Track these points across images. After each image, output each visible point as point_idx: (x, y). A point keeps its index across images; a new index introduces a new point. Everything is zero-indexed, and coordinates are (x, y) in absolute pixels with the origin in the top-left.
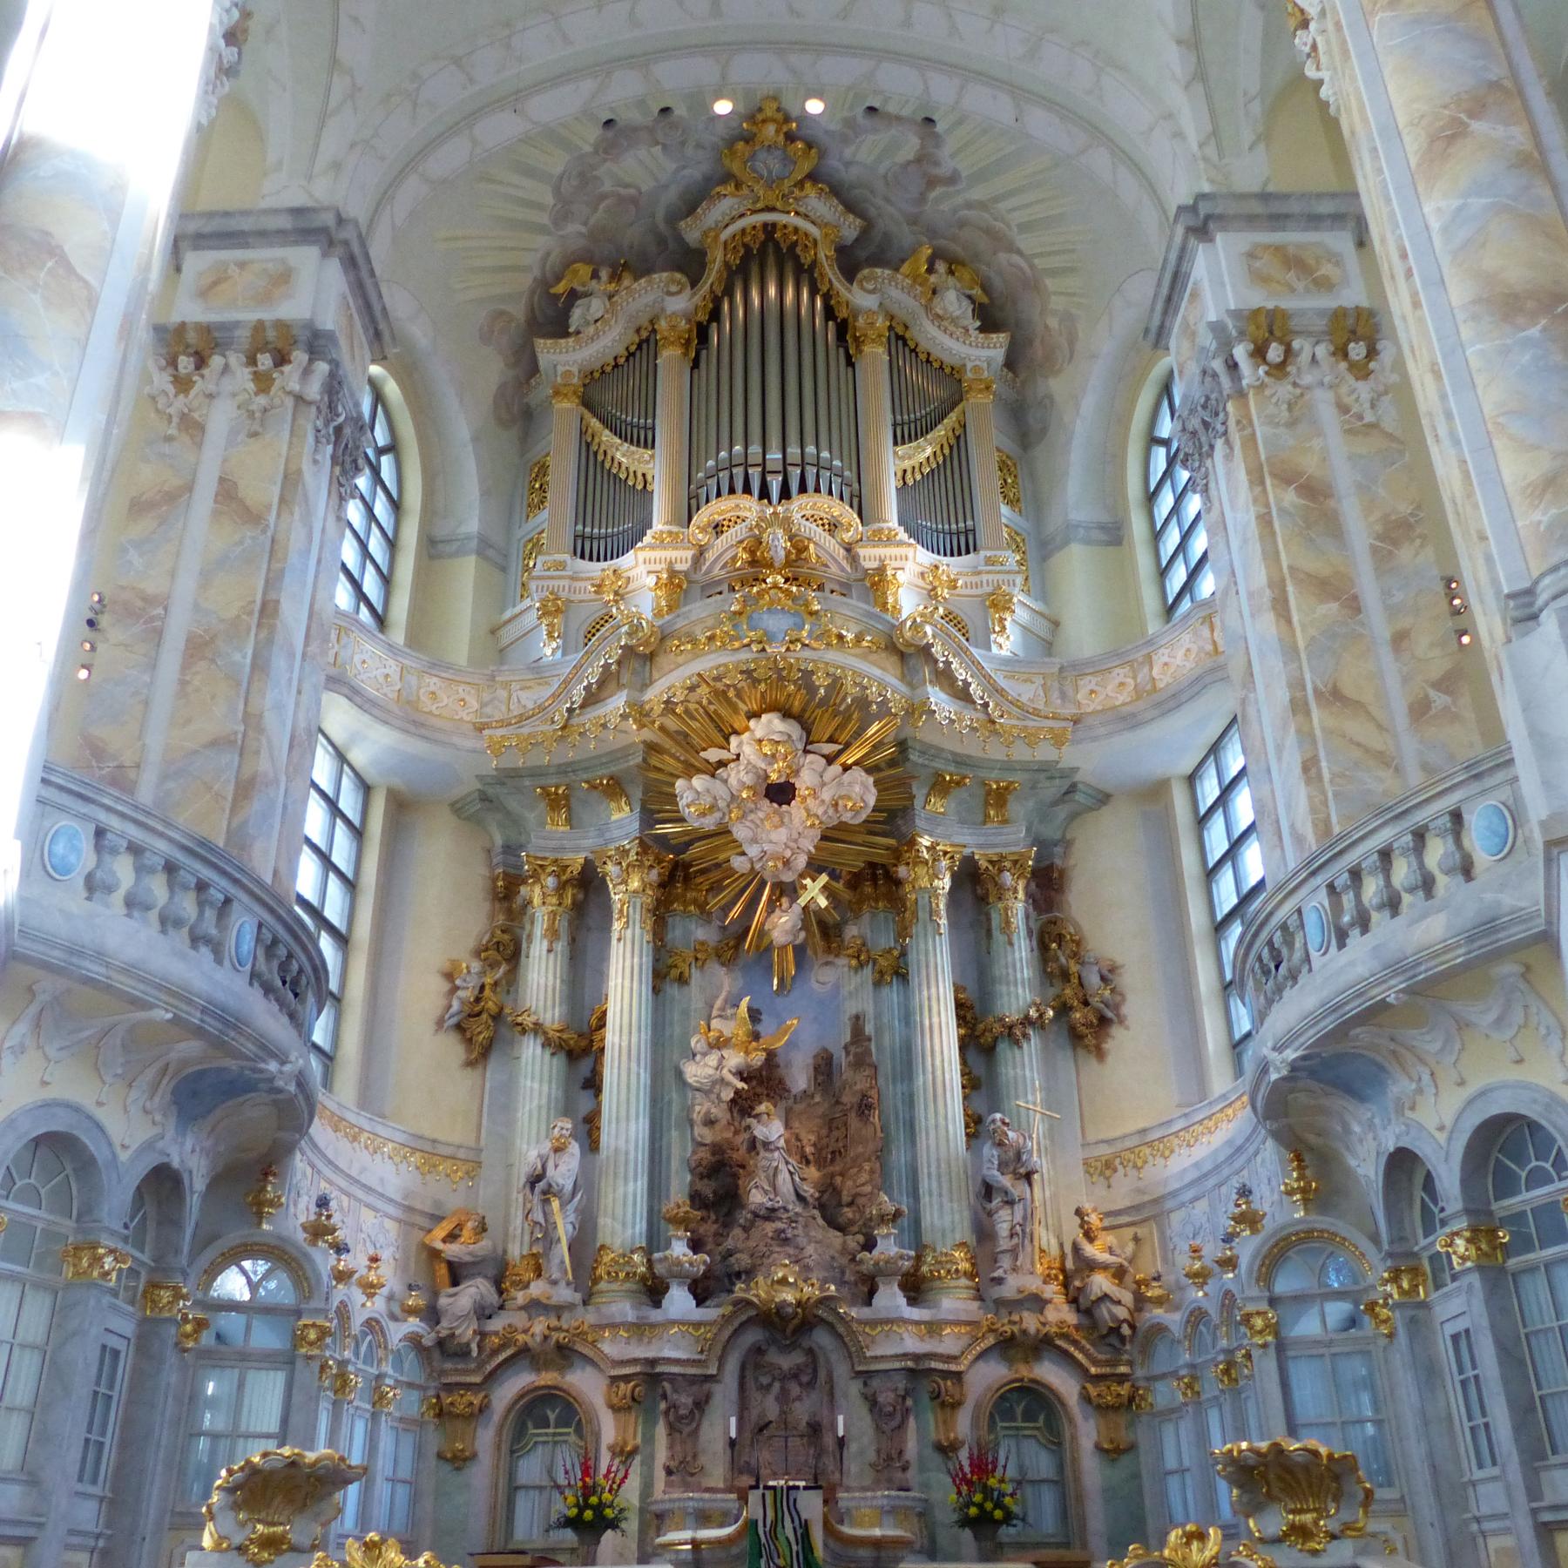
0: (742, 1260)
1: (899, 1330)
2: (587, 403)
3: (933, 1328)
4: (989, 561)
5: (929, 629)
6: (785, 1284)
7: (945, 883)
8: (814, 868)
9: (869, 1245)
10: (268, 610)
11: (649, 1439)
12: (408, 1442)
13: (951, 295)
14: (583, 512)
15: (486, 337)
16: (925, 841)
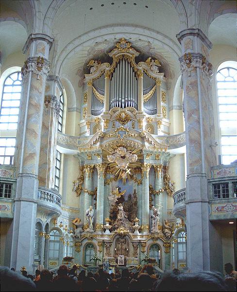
0: (117, 226)
1: (139, 237)
2: (93, 85)
3: (142, 236)
4: (158, 116)
5: (145, 134)
6: (122, 230)
7: (148, 170)
8: (129, 168)
9: (134, 225)
10: (50, 142)
11: (103, 250)
12: (72, 249)
13: (154, 67)
14: (92, 105)
15: (77, 74)
16: (145, 164)
